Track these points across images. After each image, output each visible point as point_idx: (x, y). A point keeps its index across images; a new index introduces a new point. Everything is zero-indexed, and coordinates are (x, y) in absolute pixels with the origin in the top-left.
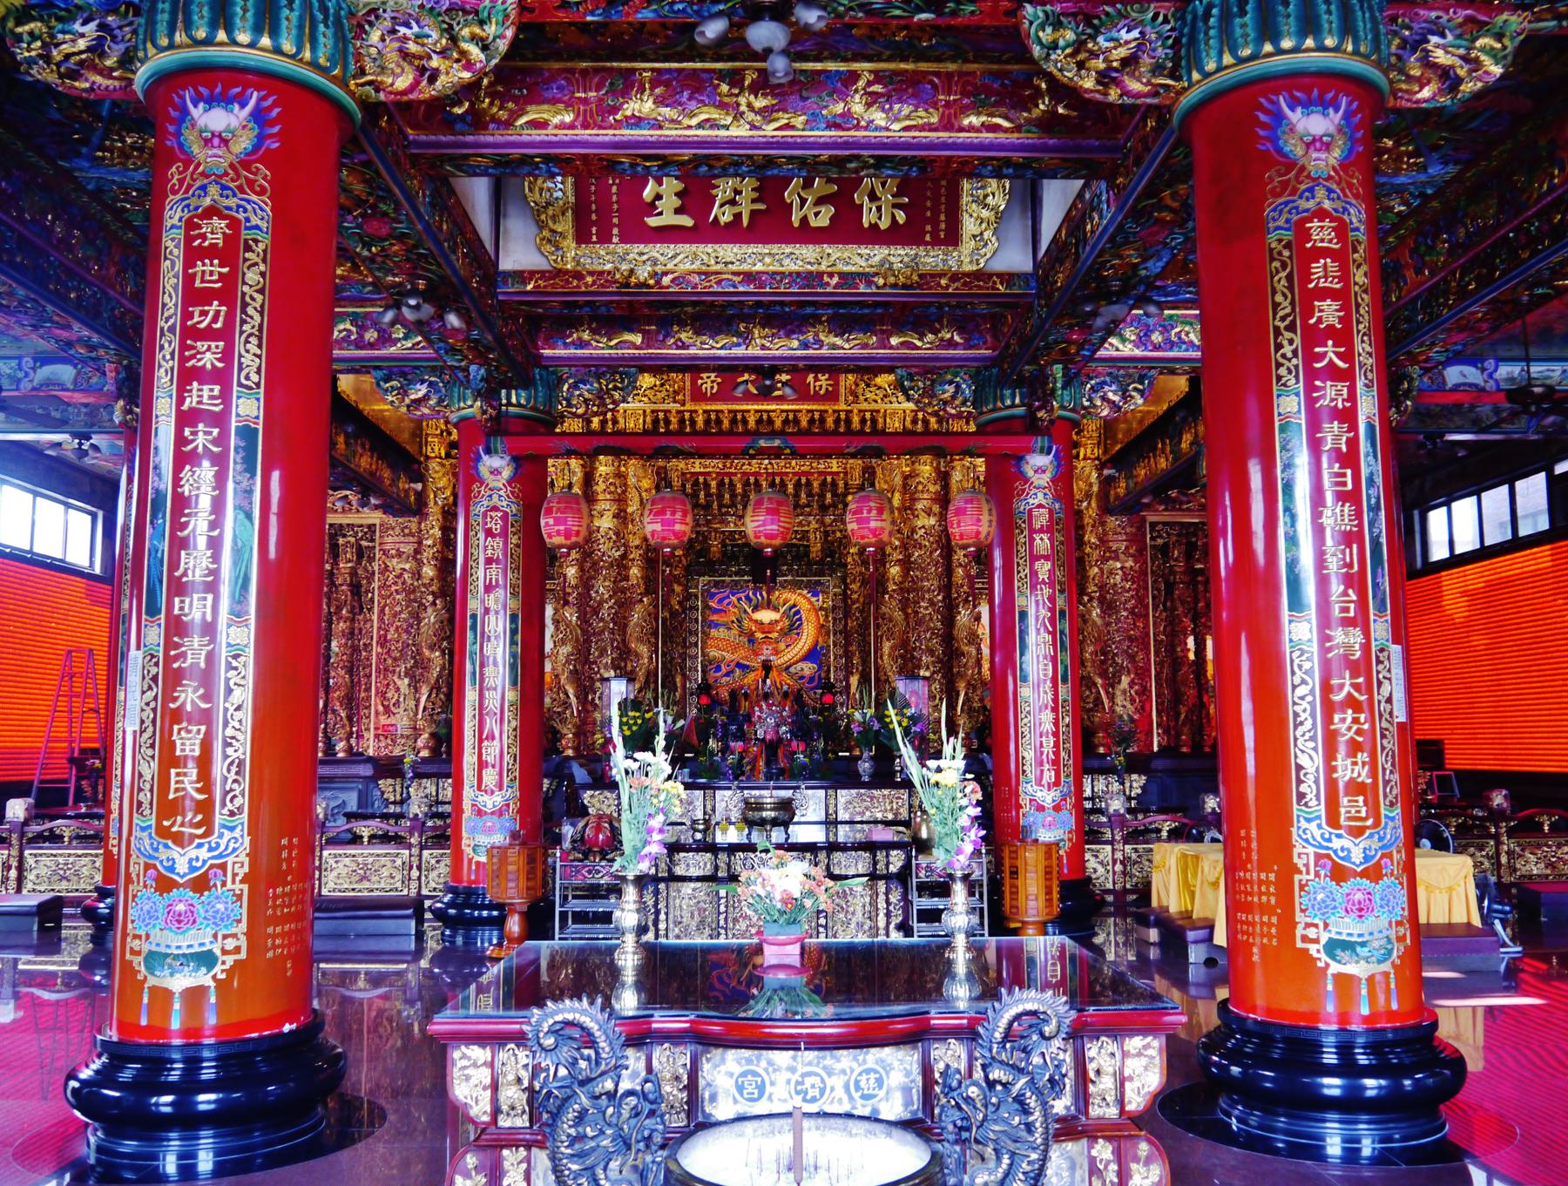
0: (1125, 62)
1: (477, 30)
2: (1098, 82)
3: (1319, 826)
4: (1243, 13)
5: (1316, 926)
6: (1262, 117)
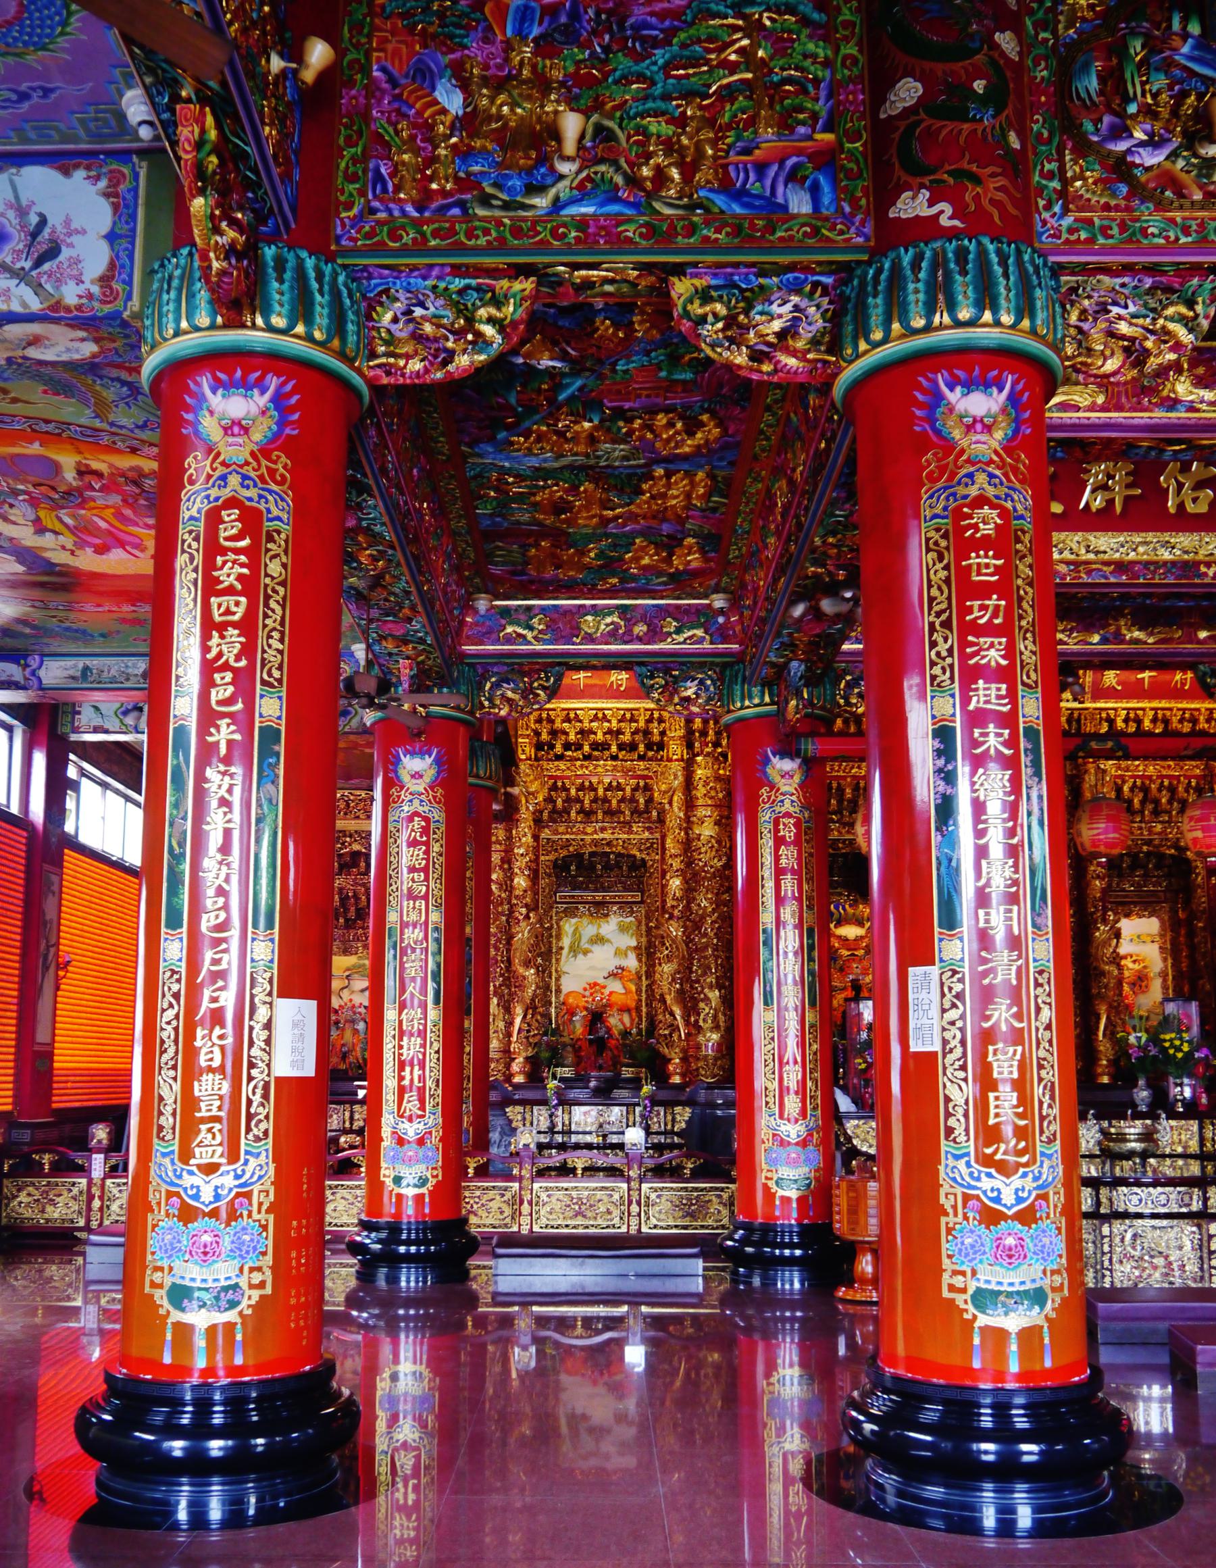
0: (782, 335)
3: (968, 1165)
5: (963, 1273)
6: (920, 397)
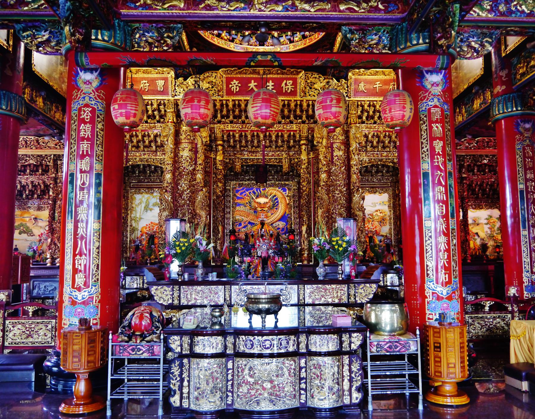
3: (433, 284)
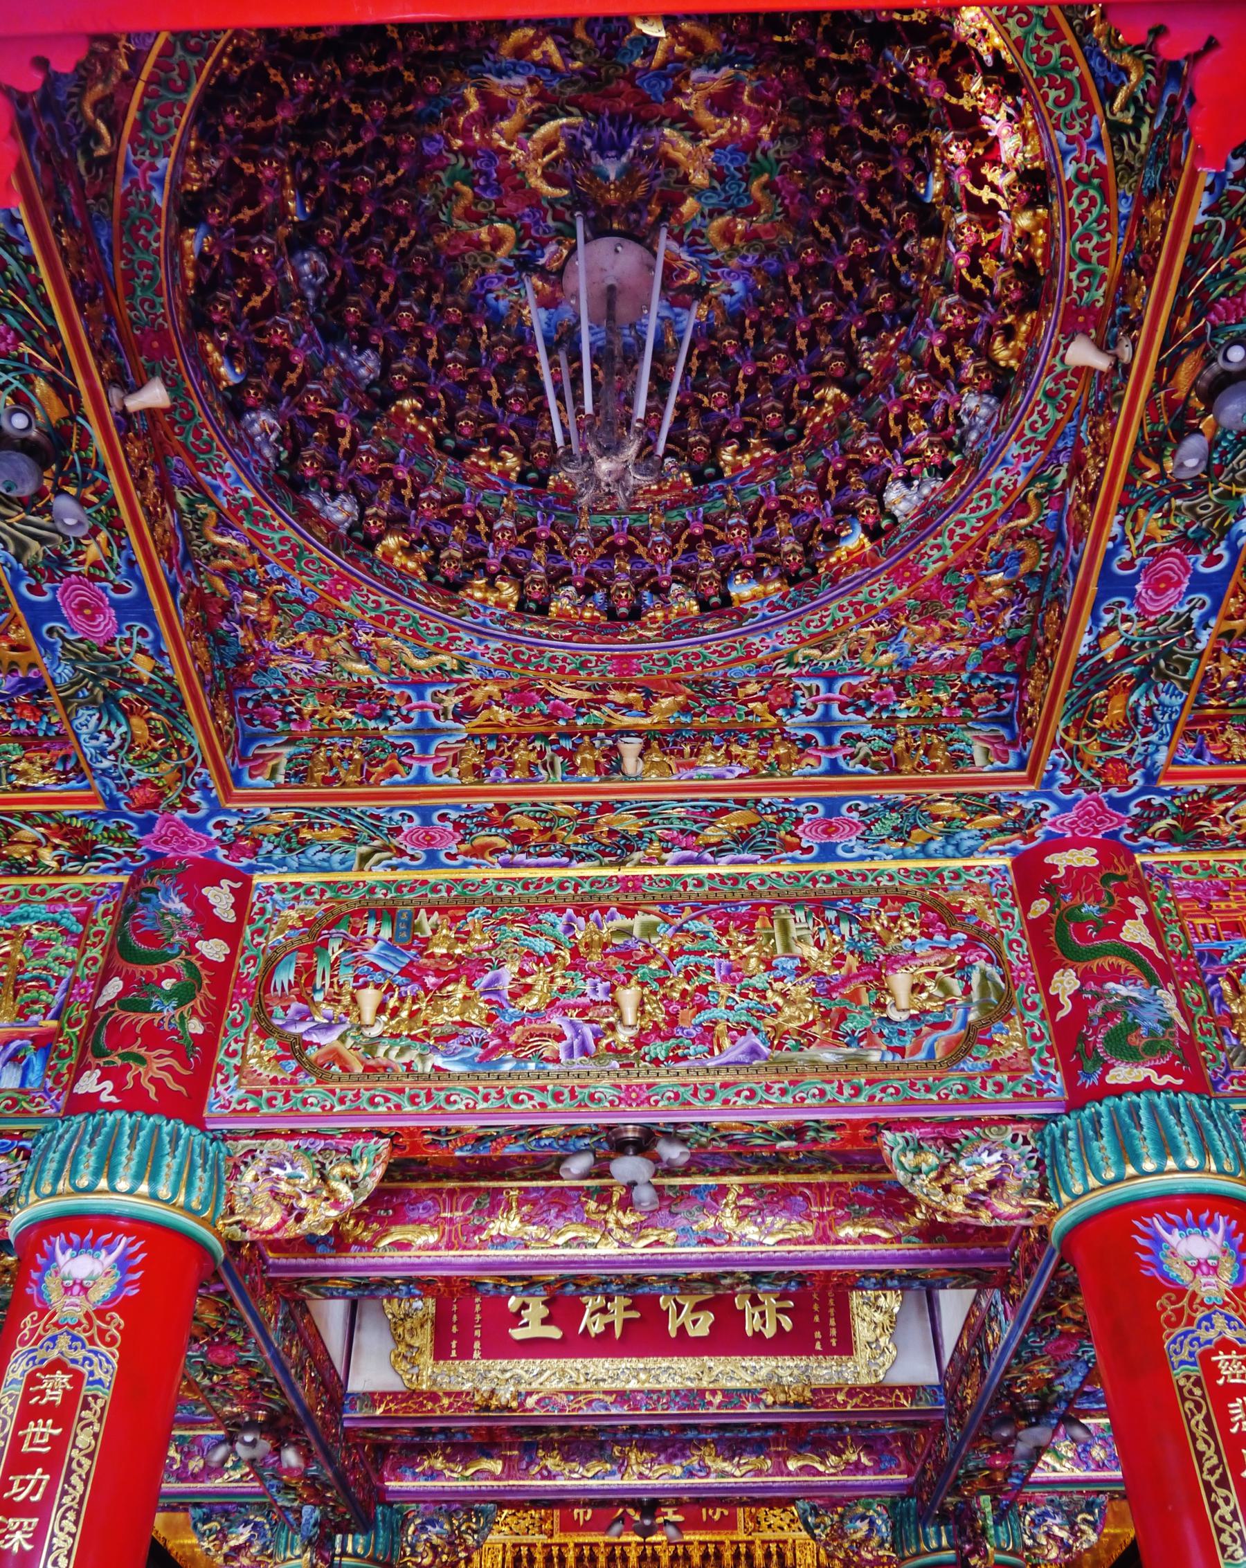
0: (992, 1184)
1: (349, 1169)
2: (968, 1206)
4: (1099, 1136)
